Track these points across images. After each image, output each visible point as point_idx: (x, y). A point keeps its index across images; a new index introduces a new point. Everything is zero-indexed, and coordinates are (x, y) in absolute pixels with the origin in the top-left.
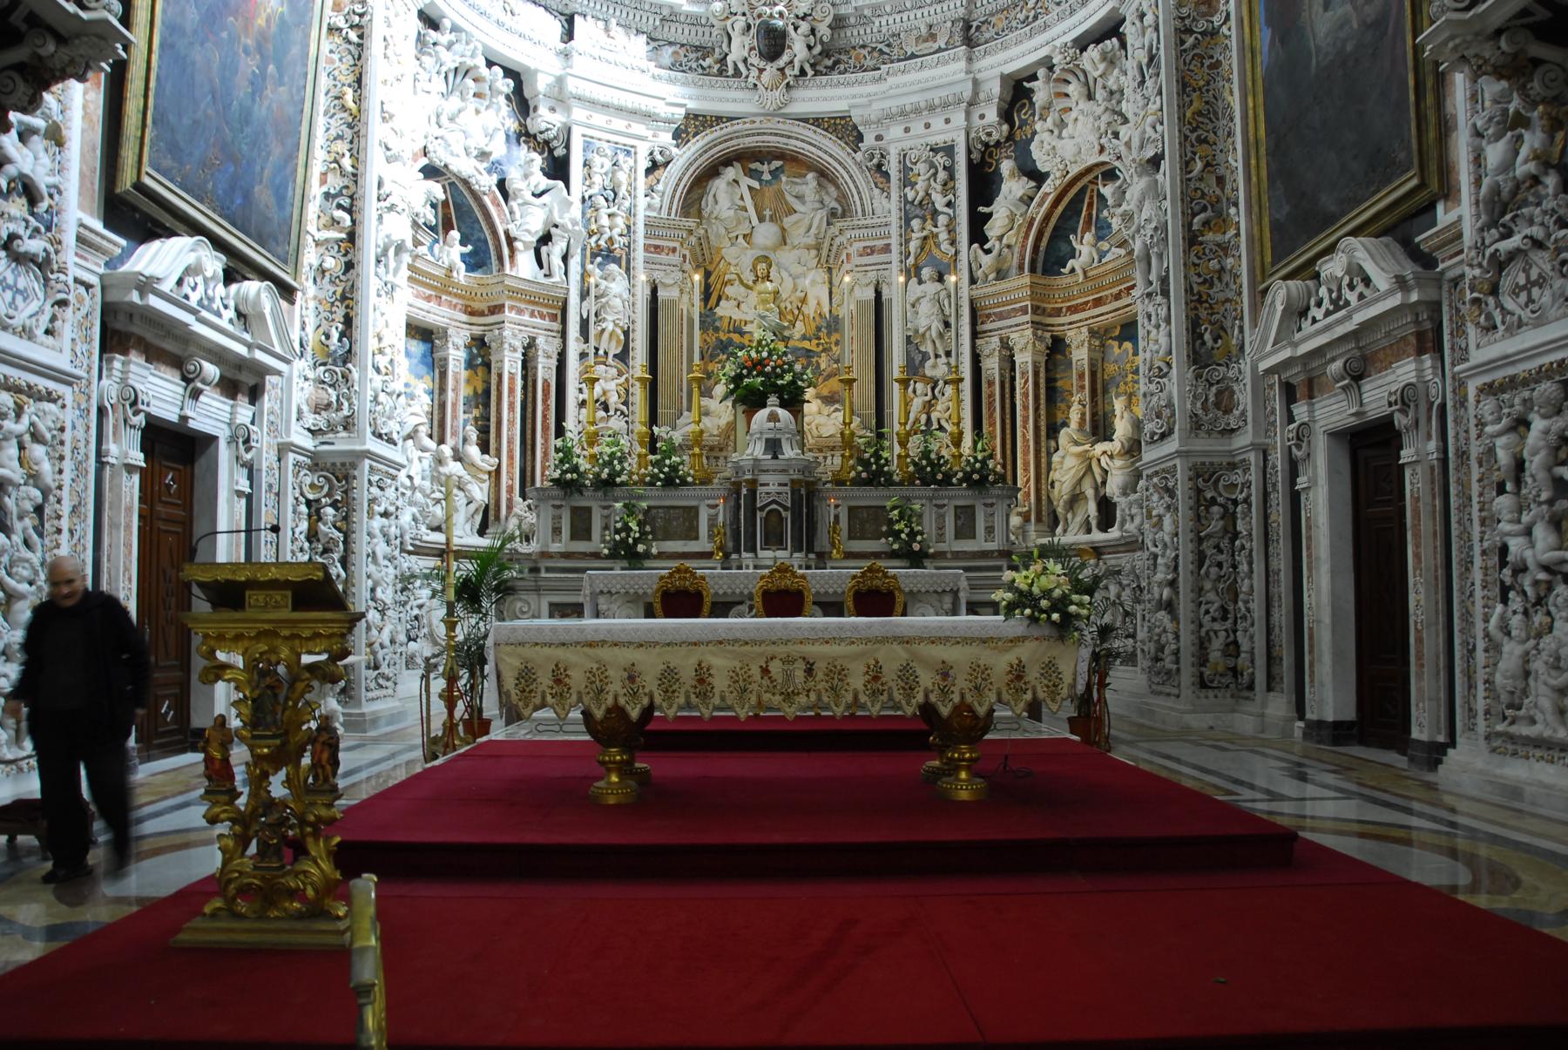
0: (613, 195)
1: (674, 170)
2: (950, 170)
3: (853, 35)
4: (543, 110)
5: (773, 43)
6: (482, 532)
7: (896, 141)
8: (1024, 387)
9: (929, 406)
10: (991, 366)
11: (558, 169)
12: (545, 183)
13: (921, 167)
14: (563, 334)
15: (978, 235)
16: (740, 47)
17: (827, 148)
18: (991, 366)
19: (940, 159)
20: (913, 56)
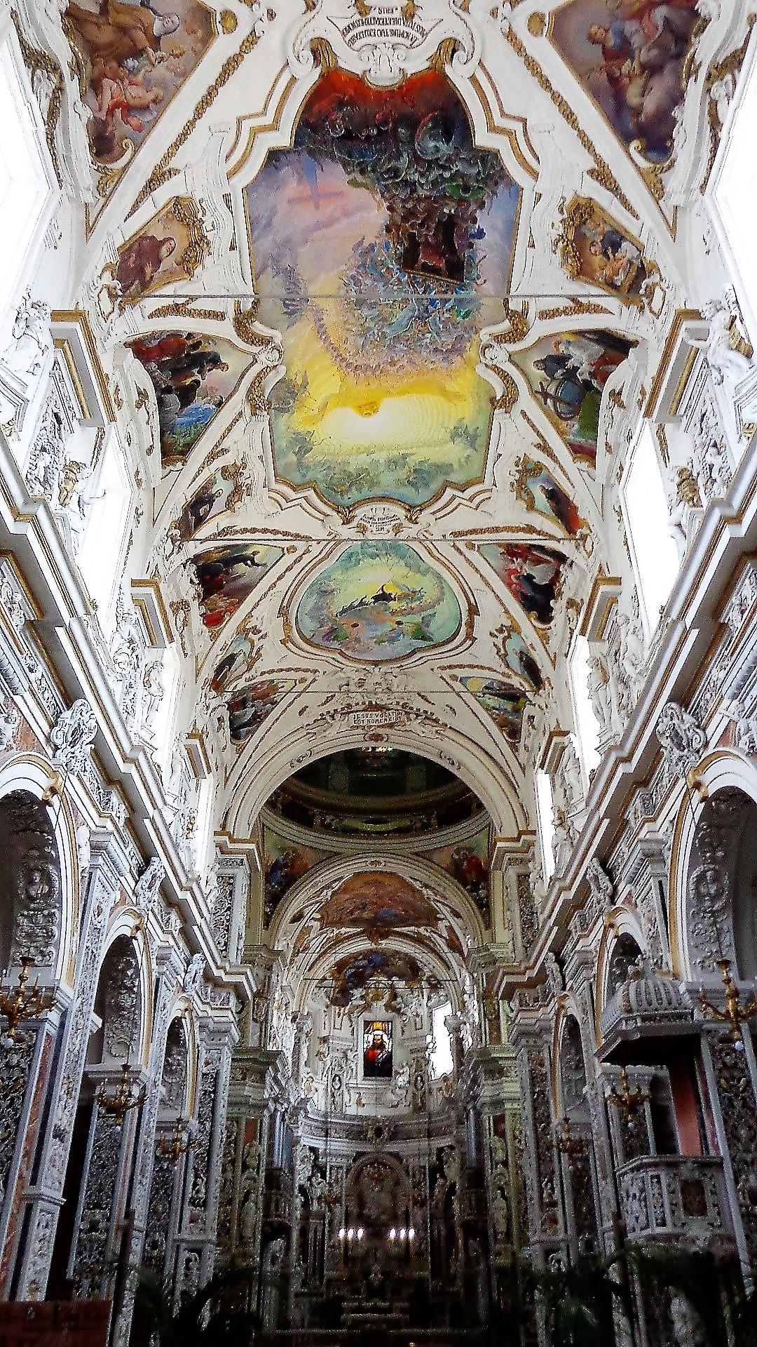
1: (352, 1171)
2: (425, 1174)
5: (378, 1132)
7: (413, 1162)
10: (436, 1232)
11: (324, 1177)
12: (320, 1180)
14: (324, 1224)
17: (392, 1161)
18: (436, 1232)
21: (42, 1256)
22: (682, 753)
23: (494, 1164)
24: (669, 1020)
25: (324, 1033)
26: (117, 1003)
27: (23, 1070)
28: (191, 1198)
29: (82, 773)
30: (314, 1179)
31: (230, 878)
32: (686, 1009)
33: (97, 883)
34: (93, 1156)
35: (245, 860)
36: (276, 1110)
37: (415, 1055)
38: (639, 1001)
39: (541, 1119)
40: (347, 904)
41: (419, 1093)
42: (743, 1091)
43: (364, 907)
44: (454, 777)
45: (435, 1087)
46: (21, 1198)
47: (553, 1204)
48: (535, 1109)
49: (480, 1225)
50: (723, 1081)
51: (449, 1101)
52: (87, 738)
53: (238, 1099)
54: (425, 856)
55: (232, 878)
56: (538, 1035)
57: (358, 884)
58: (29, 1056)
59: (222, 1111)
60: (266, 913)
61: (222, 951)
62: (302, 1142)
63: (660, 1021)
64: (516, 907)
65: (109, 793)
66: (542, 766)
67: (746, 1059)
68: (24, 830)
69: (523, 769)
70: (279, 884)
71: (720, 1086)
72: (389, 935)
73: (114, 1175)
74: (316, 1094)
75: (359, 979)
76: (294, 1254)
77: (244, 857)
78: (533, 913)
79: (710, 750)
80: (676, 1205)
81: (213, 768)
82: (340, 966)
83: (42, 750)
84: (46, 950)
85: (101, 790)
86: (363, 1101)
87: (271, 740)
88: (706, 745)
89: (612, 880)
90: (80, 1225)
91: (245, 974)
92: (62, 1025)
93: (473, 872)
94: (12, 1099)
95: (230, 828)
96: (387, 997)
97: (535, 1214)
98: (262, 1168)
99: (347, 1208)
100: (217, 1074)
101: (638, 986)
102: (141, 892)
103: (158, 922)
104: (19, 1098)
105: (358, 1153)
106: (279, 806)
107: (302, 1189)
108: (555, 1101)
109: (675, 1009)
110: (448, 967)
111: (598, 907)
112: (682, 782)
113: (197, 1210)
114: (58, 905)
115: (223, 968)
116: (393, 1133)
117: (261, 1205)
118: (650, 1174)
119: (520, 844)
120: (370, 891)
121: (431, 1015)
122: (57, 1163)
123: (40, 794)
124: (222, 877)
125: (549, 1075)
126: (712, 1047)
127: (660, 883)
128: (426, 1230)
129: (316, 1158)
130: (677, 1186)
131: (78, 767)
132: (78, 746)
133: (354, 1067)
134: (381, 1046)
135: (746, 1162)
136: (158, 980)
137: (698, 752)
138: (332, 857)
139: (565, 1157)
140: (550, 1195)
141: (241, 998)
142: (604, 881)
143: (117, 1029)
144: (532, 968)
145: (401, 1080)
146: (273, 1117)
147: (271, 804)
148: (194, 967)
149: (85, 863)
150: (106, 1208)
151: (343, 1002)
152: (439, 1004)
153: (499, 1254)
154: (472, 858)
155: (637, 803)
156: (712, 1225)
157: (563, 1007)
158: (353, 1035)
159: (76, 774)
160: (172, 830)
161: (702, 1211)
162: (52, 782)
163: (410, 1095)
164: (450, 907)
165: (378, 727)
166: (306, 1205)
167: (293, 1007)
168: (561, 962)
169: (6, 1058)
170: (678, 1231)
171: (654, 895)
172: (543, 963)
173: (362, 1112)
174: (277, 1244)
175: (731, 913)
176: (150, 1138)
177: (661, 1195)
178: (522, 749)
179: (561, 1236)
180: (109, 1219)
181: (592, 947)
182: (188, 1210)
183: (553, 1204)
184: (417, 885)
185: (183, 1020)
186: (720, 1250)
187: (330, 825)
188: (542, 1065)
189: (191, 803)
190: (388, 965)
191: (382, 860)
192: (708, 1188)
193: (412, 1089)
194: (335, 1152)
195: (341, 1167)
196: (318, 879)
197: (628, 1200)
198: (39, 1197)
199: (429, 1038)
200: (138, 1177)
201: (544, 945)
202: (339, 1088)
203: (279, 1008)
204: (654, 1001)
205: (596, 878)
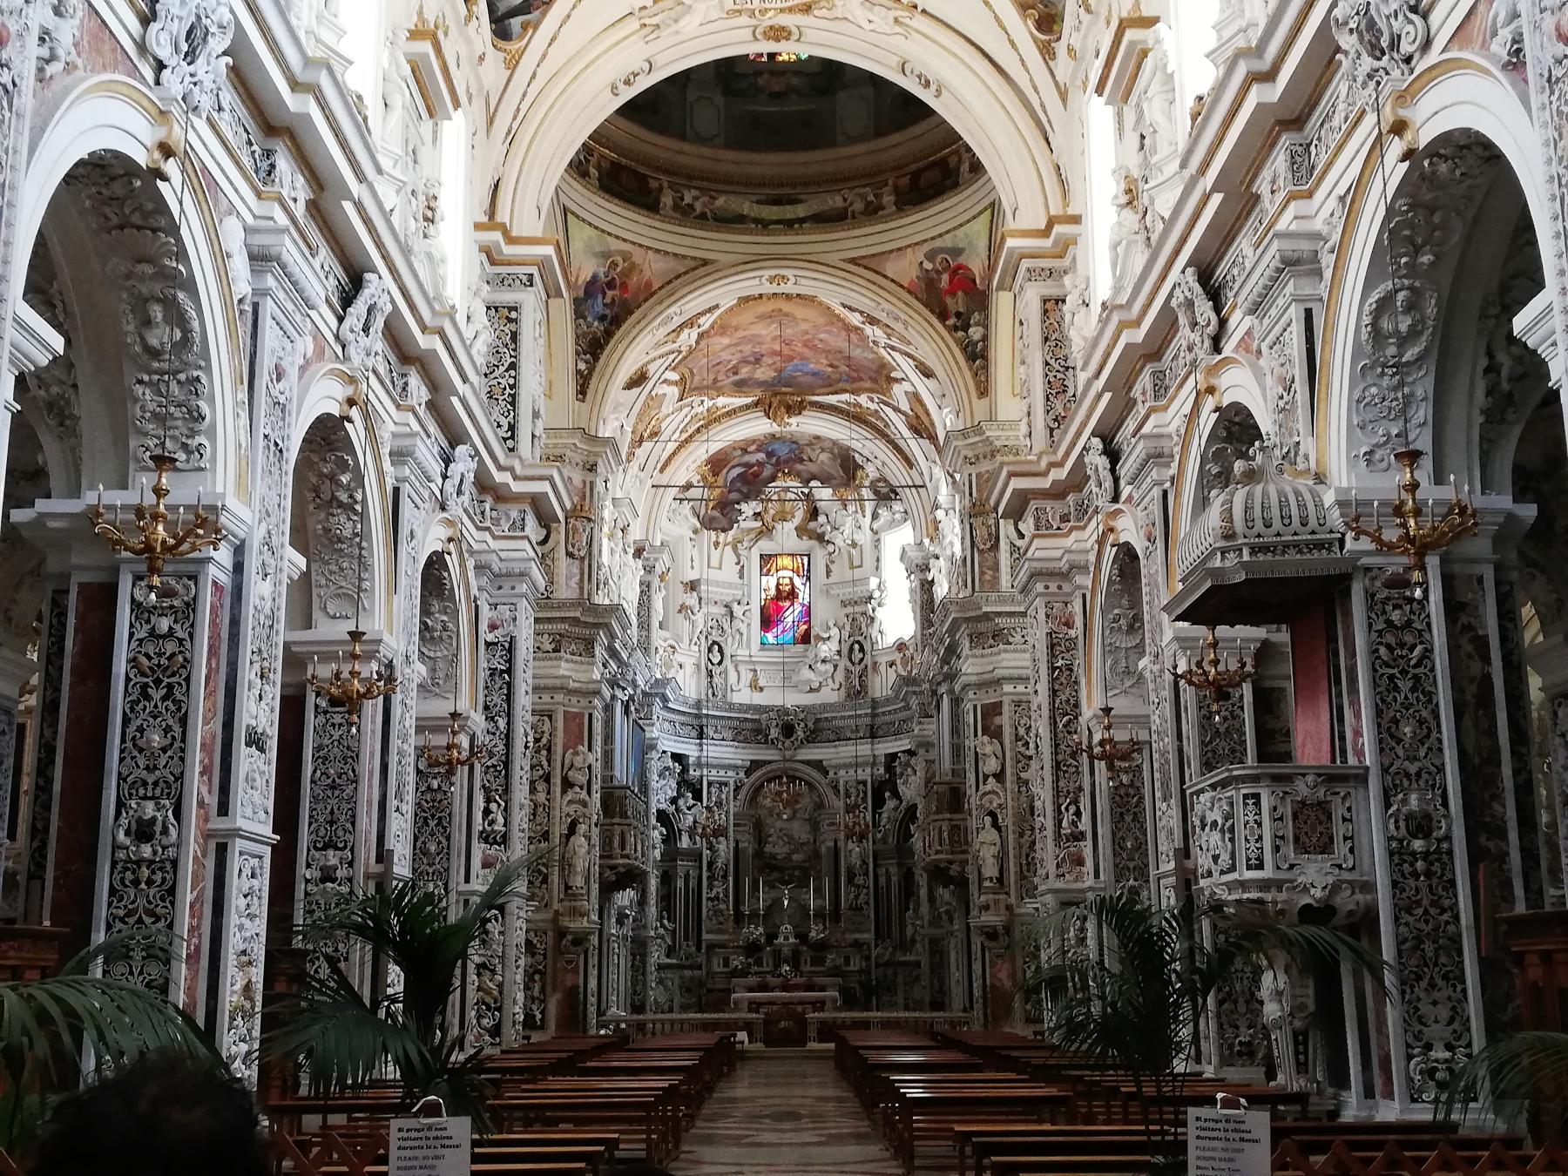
0: (719, 804)
2: (865, 792)
3: (825, 725)
4: (691, 772)
5: (788, 730)
6: (668, 956)
8: (894, 890)
9: (857, 897)
10: (882, 880)
11: (698, 796)
12: (691, 802)
13: (853, 790)
14: (701, 868)
15: (876, 824)
16: (774, 733)
18: (882, 880)
19: (861, 787)
20: (850, 739)
21: (251, 917)
22: (1376, 64)
23: (981, 778)
24: (1300, 552)
25: (692, 575)
26: (327, 530)
27: (181, 641)
28: (482, 832)
29: (215, 115)
30: (681, 802)
31: (511, 309)
32: (1331, 532)
33: (269, 320)
34: (315, 771)
35: (537, 278)
36: (613, 697)
37: (849, 610)
38: (1249, 521)
39: (1064, 710)
40: (725, 356)
41: (857, 669)
42: (1415, 667)
43: (758, 360)
44: (928, 112)
45: (883, 660)
46: (207, 835)
47: (1080, 837)
48: (1054, 693)
49: (955, 868)
50: (1383, 650)
51: (908, 681)
52: (218, 44)
53: (550, 682)
54: (868, 266)
55: (516, 309)
56: (1065, 576)
57: (747, 316)
58: (188, 618)
59: (524, 700)
60: (578, 372)
61: (505, 439)
62: (661, 747)
63: (1284, 552)
64: (1036, 357)
65: (268, 153)
66: (1099, 90)
67: (1428, 616)
68: (121, 227)
69: (1063, 95)
70: (602, 318)
72: (805, 408)
73: (352, 800)
74: (681, 672)
75: (751, 483)
76: (652, 910)
77: (534, 270)
78: (1067, 368)
79: (1434, 56)
80: (1282, 838)
81: (463, 98)
82: (717, 463)
83: (134, 71)
84: (193, 443)
85: (255, 147)
86: (761, 683)
87: (571, 40)
88: (1427, 44)
89: (1218, 309)
90: (302, 871)
91: (550, 479)
92: (238, 568)
93: (960, 293)
94: (170, 687)
95: (503, 216)
96: (799, 515)
97: (1047, 852)
98: (596, 786)
99: (737, 842)
100: (510, 643)
101: (1249, 495)
102: (351, 337)
103: (388, 392)
104: (180, 684)
105: (752, 762)
106: (593, 171)
107: (662, 816)
108: (1089, 683)
109: (1313, 532)
110: (910, 465)
111: (1189, 357)
112: (1370, 119)
113: (493, 851)
114: (203, 364)
115: (511, 469)
116: (812, 732)
117: (596, 840)
119: (1047, 243)
120: (767, 331)
121: (877, 543)
122: (258, 783)
123: (141, 158)
124: (496, 308)
125: (1081, 638)
126: (1370, 596)
127: (1309, 314)
128: (866, 874)
129: (685, 770)
131: (206, 102)
132: (201, 61)
133: (744, 630)
134: (792, 595)
135: (1408, 775)
136: (396, 490)
137: (1408, 60)
138: (699, 269)
139: (1101, 766)
140: (1074, 824)
141: (545, 520)
142: (1204, 309)
143: (331, 572)
144: (1060, 464)
145: (826, 649)
146: (608, 709)
147: (578, 168)
148: (456, 469)
149: (243, 286)
150: (345, 847)
151: (724, 522)
152: (892, 524)
153: (986, 907)
154: (960, 267)
155: (1279, 162)
156: (1340, 867)
157: (1112, 530)
158: (741, 577)
159: (204, 116)
160: (395, 219)
161: (1326, 847)
162: (161, 133)
163: (840, 676)
164: (914, 359)
165: (782, 10)
166: (670, 838)
167: (636, 533)
168: (1113, 455)
169: (148, 621)
171: (1295, 334)
172: (1081, 456)
173: (759, 699)
174: (625, 898)
175: (1433, 368)
176: (405, 745)
177: (1260, 825)
178: (1061, 48)
179: (1089, 881)
180: (351, 864)
181: (1172, 428)
182: (478, 850)
183: (1080, 837)
184: (855, 319)
185: (447, 557)
186: (1346, 901)
187: (691, 206)
188: (1069, 624)
189: (426, 169)
190: (802, 461)
191: (788, 273)
192: (1338, 811)
193: (844, 663)
194: (715, 762)
195: (726, 784)
196: (671, 310)
197: (1203, 829)
198: (236, 833)
199: (874, 582)
200: (392, 803)
201: (1084, 424)
202: (720, 663)
203: (611, 537)
204: (1277, 525)
205: (1190, 304)
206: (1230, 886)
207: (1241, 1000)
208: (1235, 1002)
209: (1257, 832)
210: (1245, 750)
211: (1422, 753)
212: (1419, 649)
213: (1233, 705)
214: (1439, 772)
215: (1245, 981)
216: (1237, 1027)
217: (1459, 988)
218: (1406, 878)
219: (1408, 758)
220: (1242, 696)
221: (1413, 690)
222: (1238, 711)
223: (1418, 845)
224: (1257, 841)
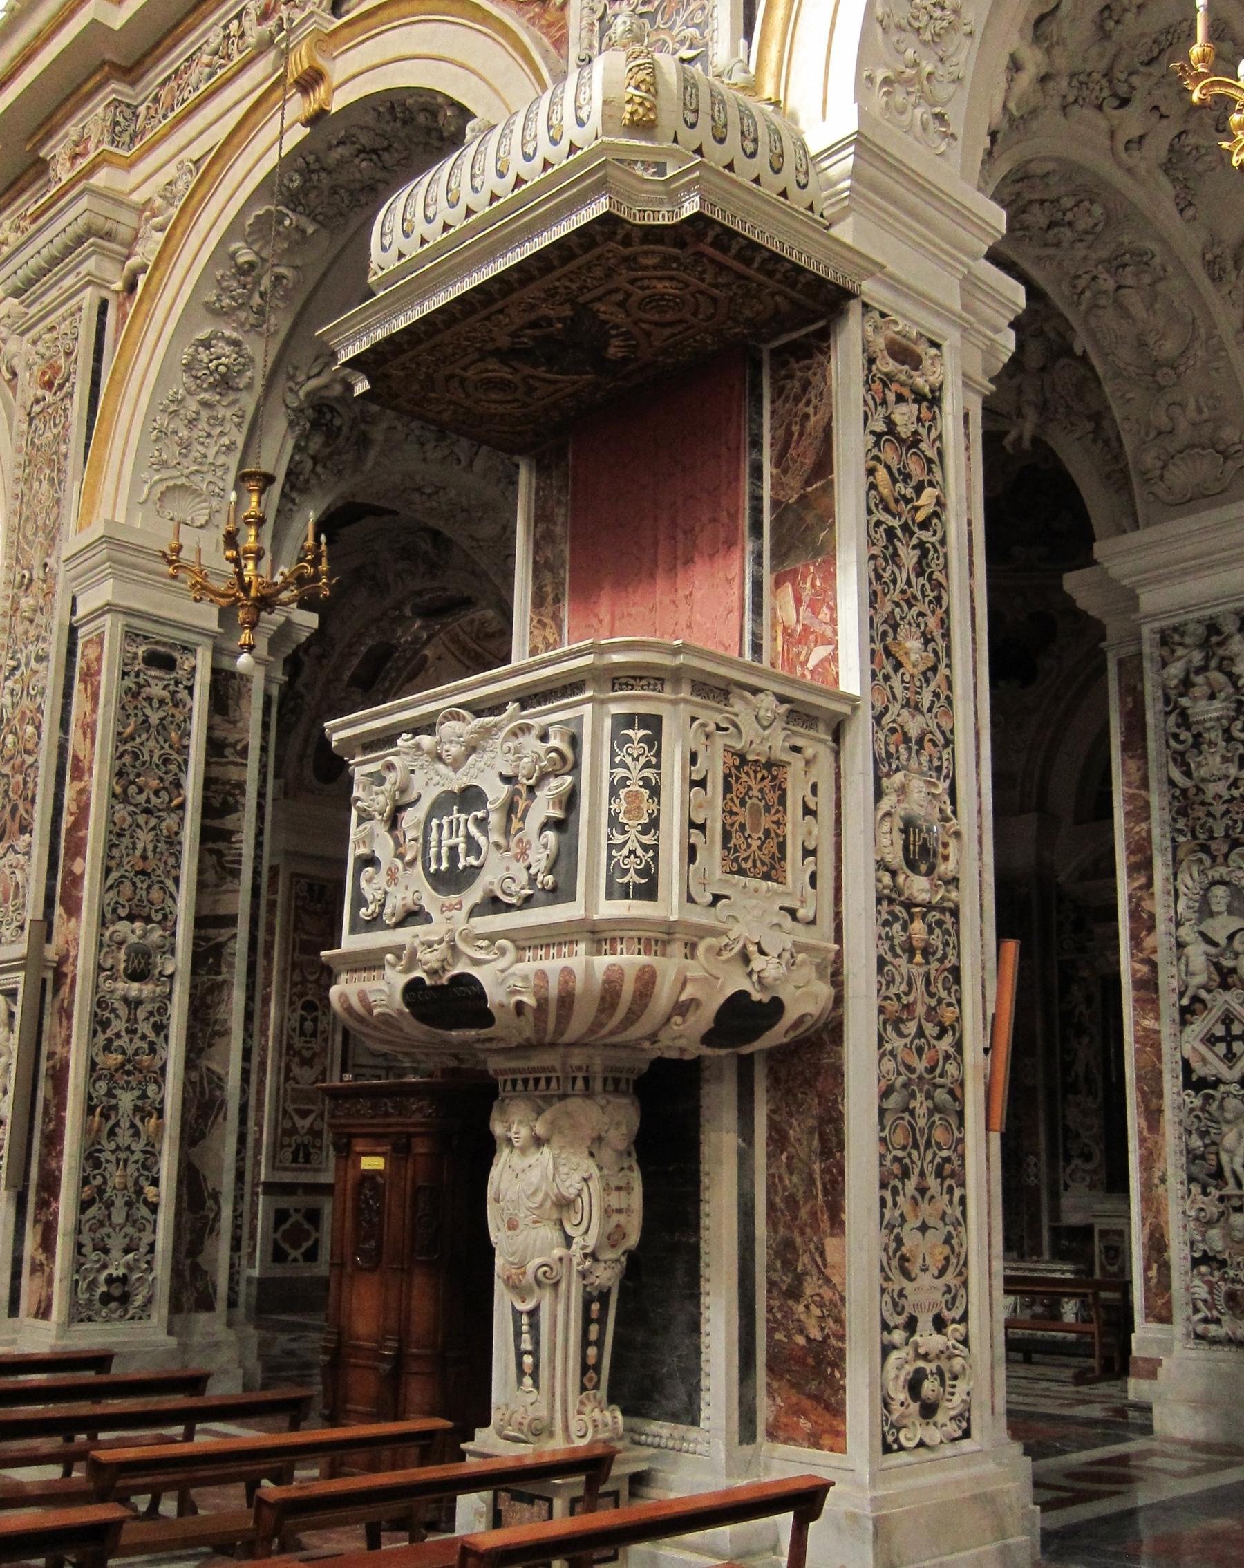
67: (940, 437)
71: (873, 486)
80: (702, 828)
118: (616, 709)
130: (715, 766)
135: (906, 739)
156: (792, 913)
161: (772, 871)
170: (699, 916)
177: (655, 791)
206: (527, 941)
207: (119, 1202)
208: (109, 1205)
209: (647, 806)
210: (186, 762)
211: (926, 701)
212: (928, 495)
213: (177, 684)
214: (946, 745)
215: (131, 1168)
216: (106, 1251)
217: (957, 1193)
218: (896, 956)
219: (907, 704)
220: (194, 668)
221: (920, 570)
222: (183, 694)
223: (919, 887)
224: (645, 830)
